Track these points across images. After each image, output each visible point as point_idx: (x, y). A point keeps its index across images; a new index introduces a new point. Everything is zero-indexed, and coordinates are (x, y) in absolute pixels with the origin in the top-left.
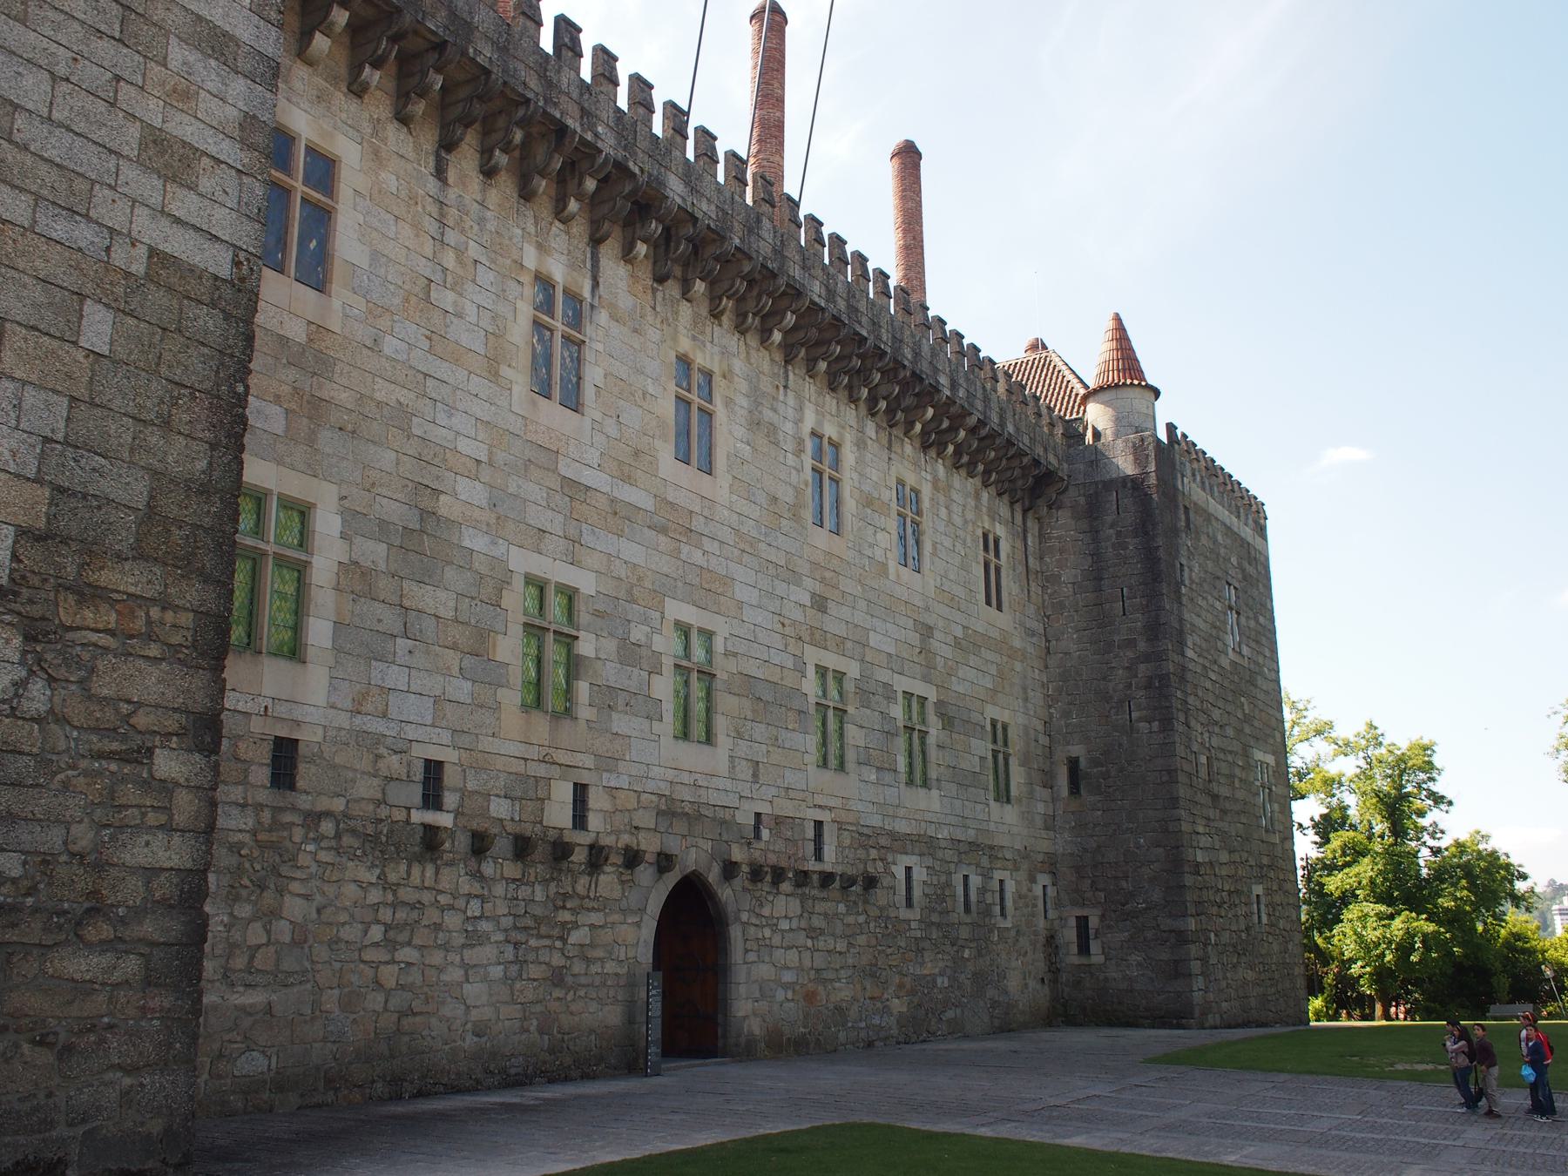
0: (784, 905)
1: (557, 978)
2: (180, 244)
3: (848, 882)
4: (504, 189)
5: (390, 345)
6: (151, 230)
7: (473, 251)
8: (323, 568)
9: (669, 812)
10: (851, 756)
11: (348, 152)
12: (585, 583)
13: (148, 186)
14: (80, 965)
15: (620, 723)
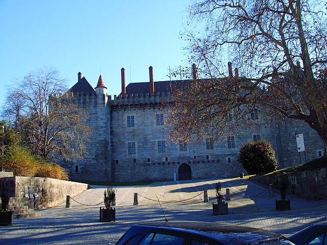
0: (201, 165)
1: (165, 174)
2: (101, 139)
3: (213, 161)
4: (152, 109)
5: (141, 128)
6: (99, 139)
7: (148, 116)
8: (136, 147)
9: (180, 158)
10: (214, 147)
11: (135, 115)
12: (165, 140)
13: (98, 137)
14: (100, 174)
15: (171, 151)
